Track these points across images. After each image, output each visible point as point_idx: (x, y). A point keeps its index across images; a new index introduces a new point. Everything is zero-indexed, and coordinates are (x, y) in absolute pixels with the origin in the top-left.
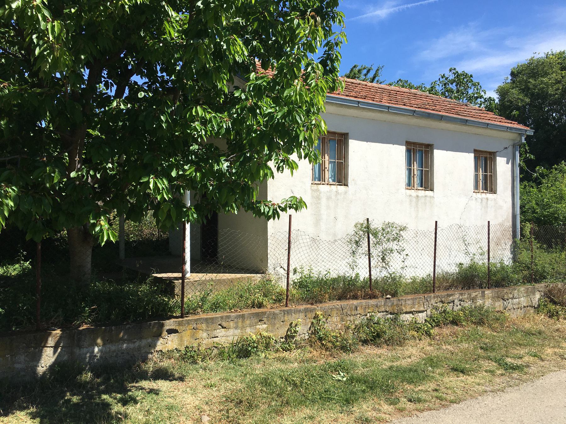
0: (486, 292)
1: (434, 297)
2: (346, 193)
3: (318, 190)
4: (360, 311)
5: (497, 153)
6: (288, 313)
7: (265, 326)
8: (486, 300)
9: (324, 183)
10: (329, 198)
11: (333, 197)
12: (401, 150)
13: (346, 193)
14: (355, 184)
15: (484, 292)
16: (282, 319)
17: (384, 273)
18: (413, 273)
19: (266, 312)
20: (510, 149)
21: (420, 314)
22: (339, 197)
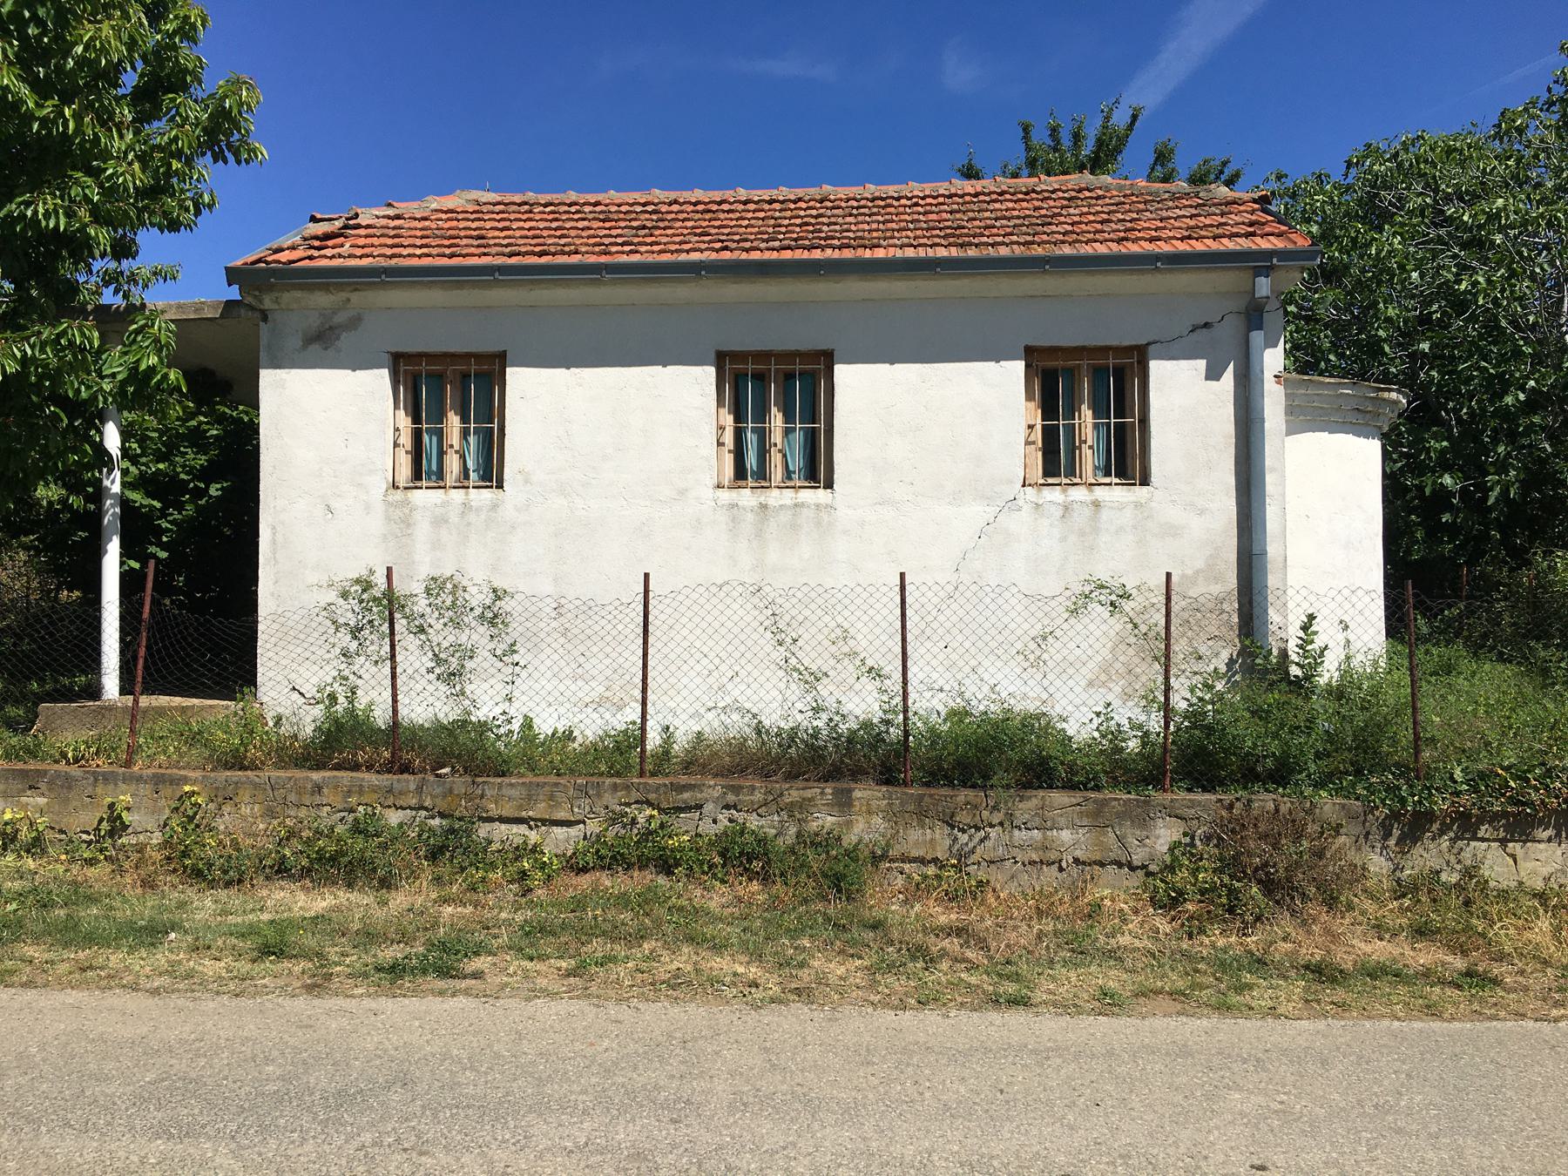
0: (857, 794)
1: (615, 787)
2: (495, 507)
3: (406, 502)
4: (328, 796)
5: (1152, 348)
6: (106, 779)
7: (42, 801)
8: (866, 818)
9: (1077, 480)
10: (439, 521)
11: (454, 518)
12: (695, 386)
13: (495, 507)
14: (527, 481)
15: (850, 791)
16: (89, 791)
17: (448, 712)
18: (599, 721)
19: (46, 772)
20: (1228, 330)
21: (557, 830)
22: (472, 517)
